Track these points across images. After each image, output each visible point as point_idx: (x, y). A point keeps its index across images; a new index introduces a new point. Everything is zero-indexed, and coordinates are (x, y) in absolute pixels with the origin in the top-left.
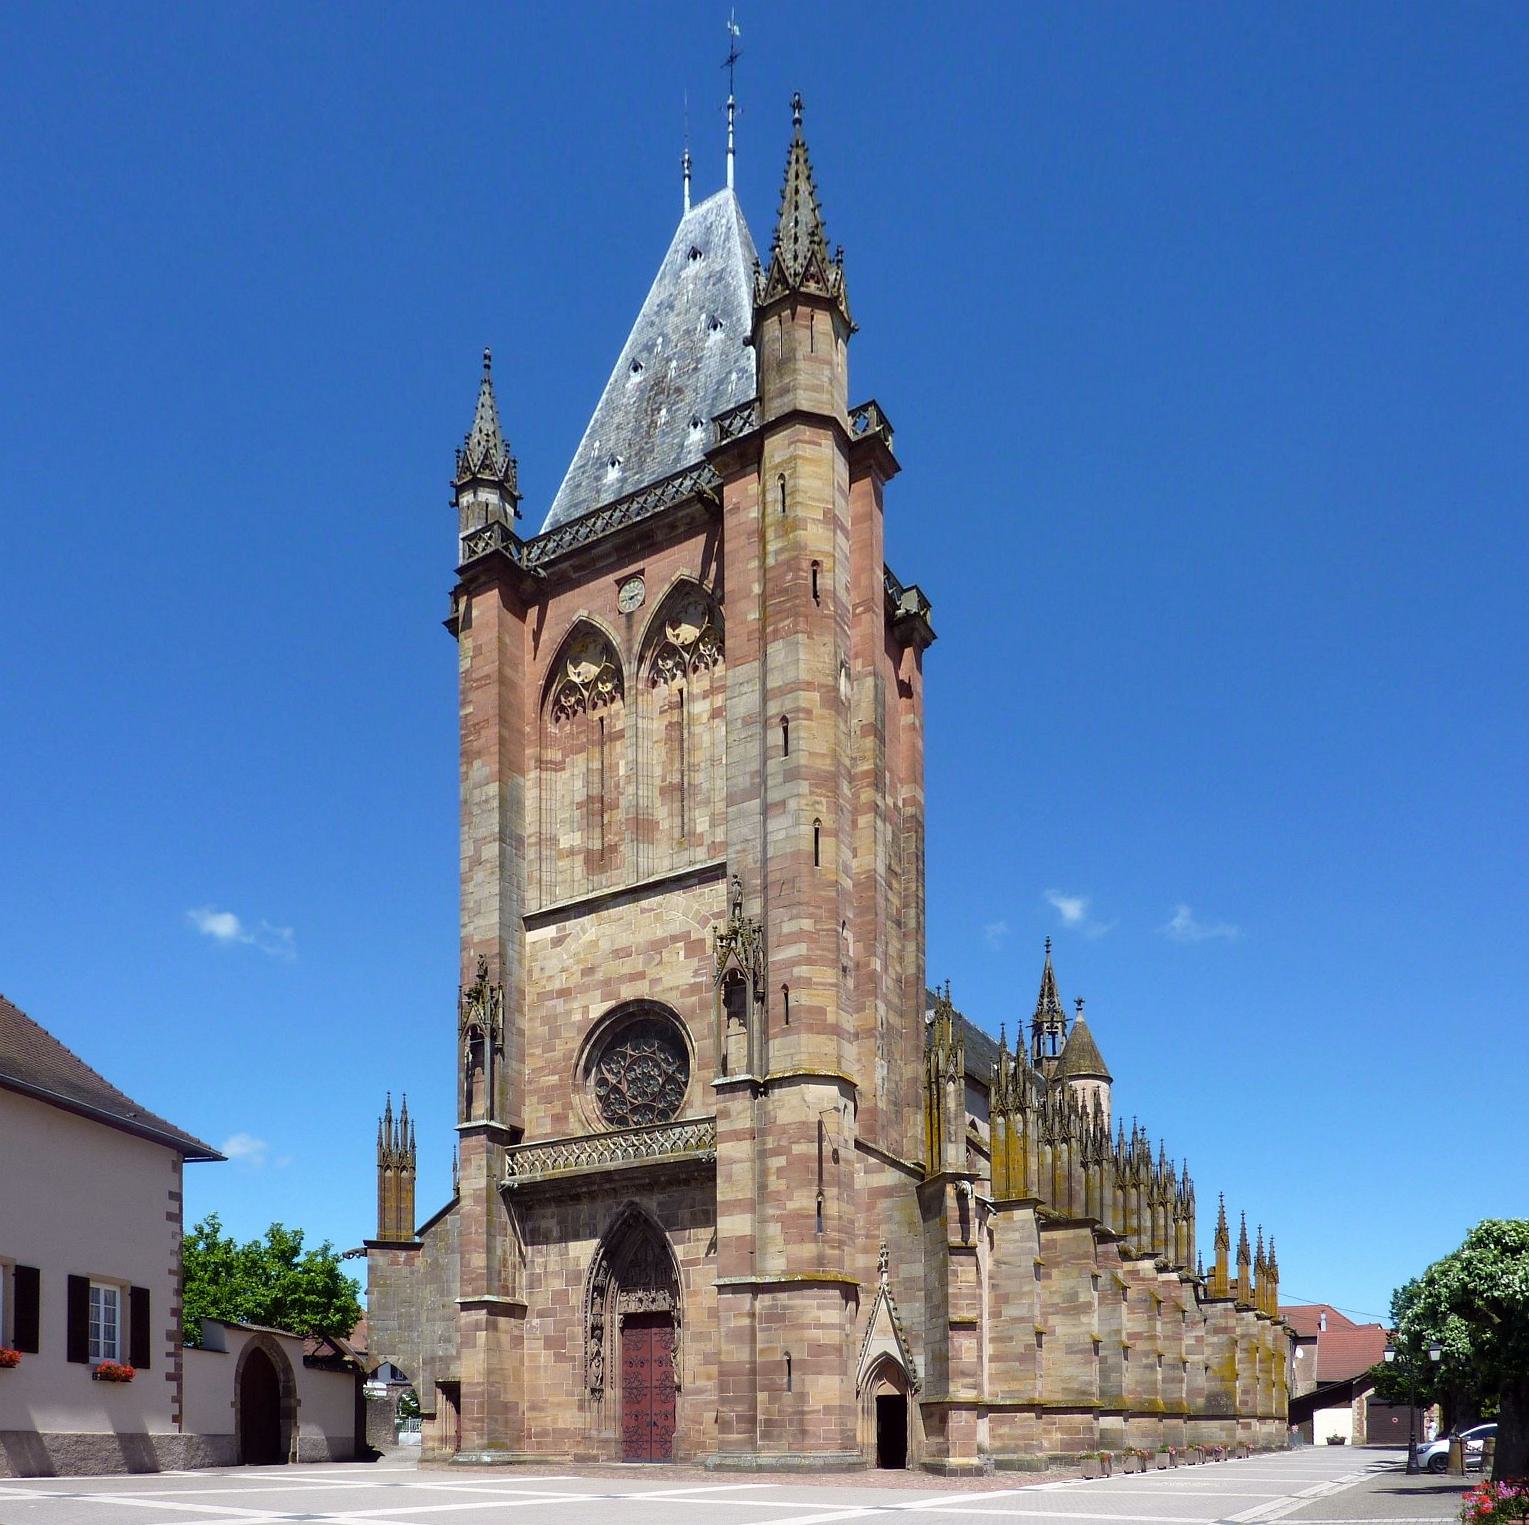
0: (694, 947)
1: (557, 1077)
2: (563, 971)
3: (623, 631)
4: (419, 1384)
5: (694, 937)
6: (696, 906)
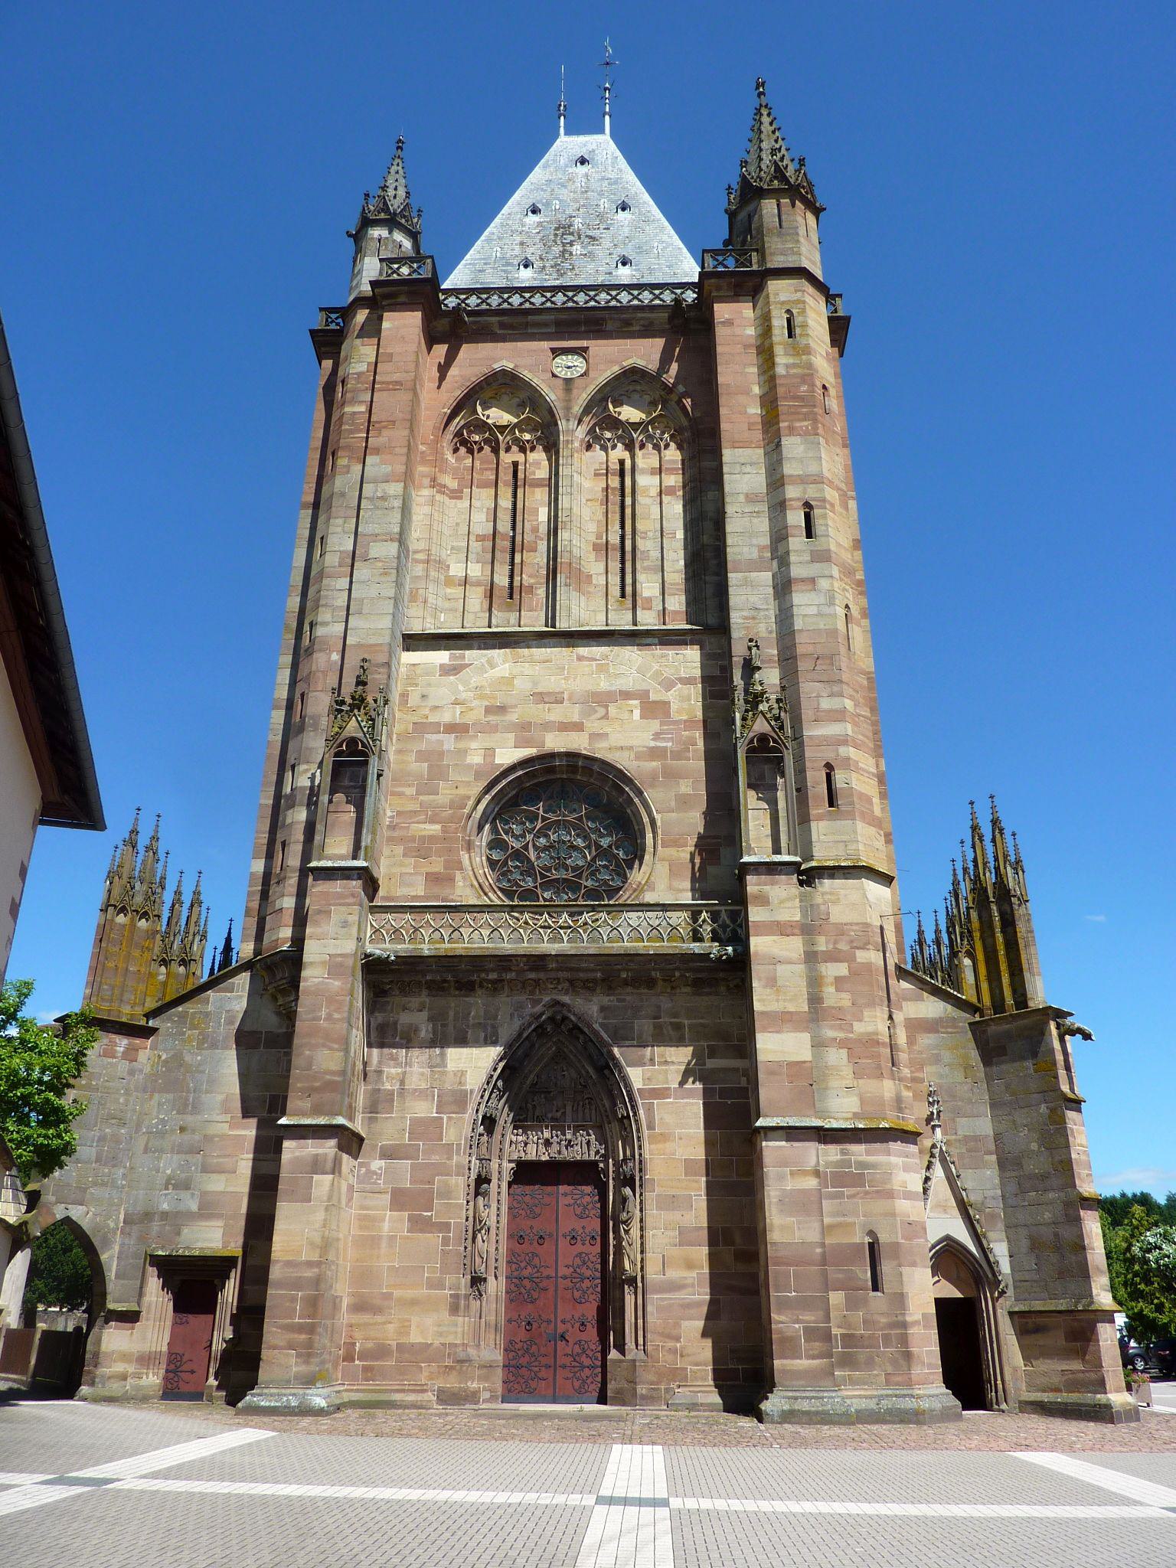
2: (456, 703)
4: (111, 1257)
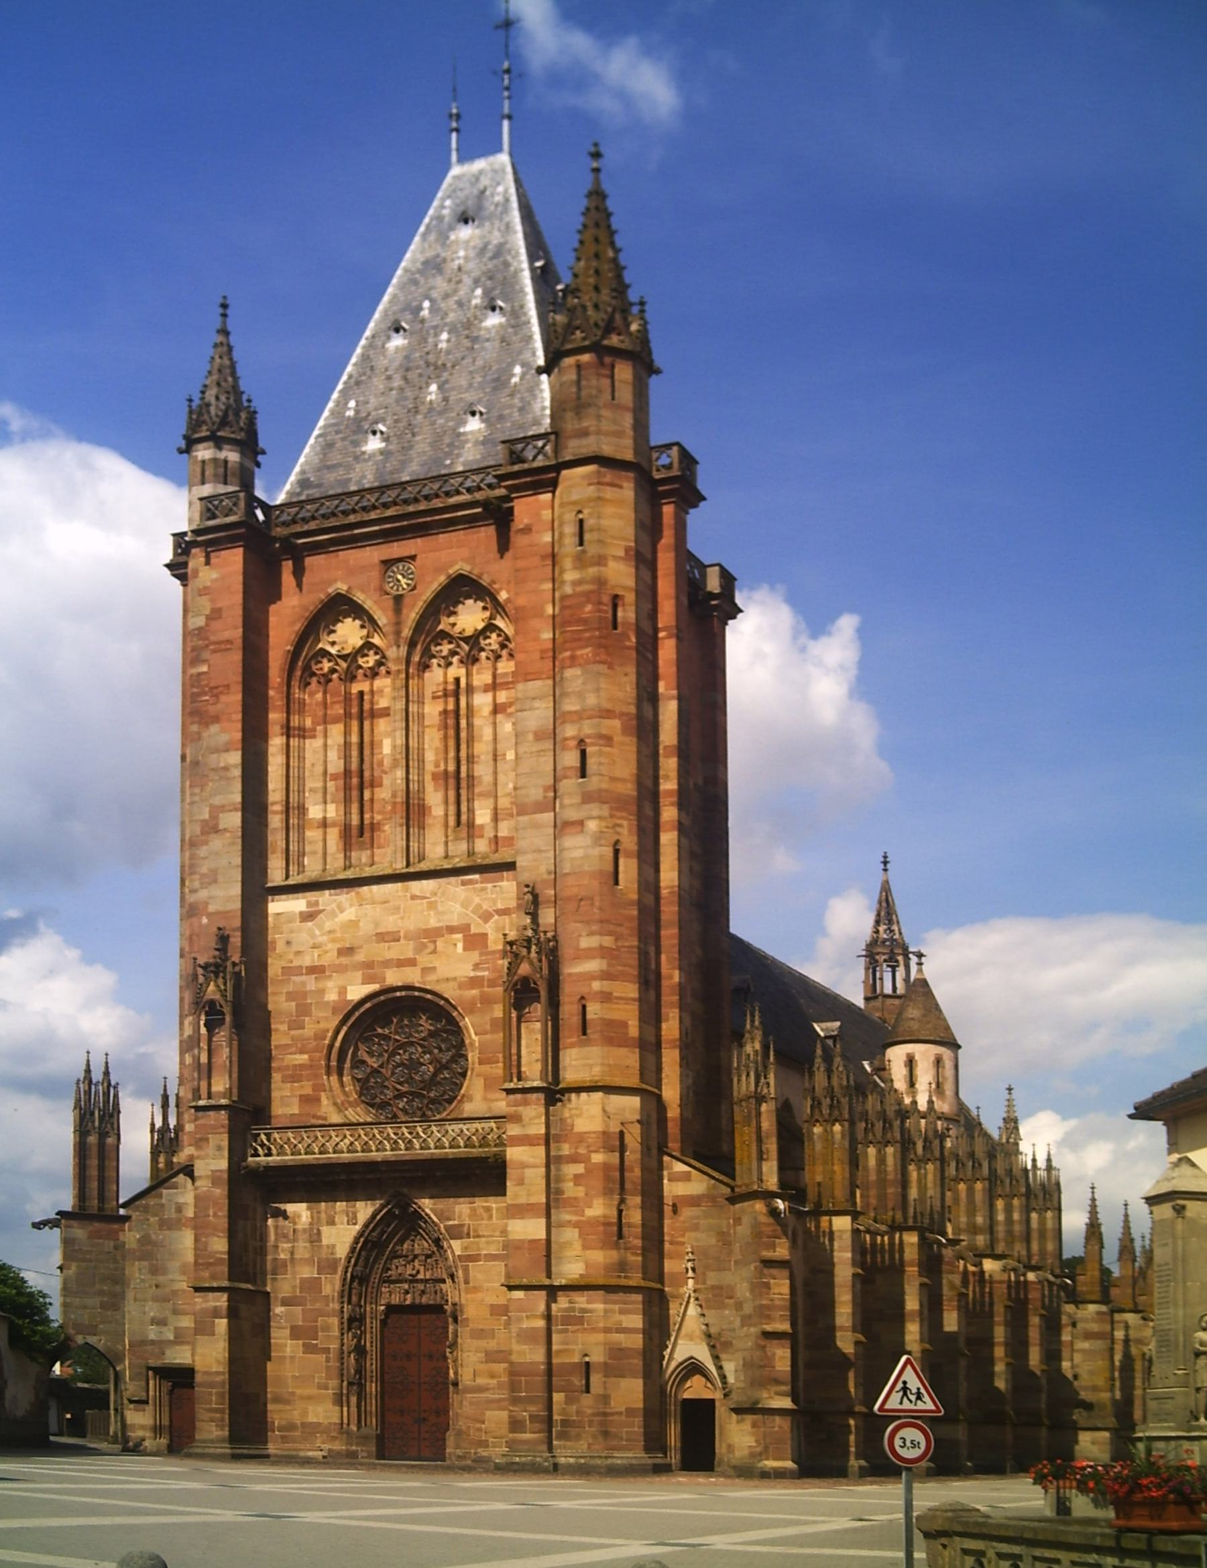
0: (475, 941)
1: (306, 1057)
3: (390, 613)
5: (473, 930)
6: (477, 900)
